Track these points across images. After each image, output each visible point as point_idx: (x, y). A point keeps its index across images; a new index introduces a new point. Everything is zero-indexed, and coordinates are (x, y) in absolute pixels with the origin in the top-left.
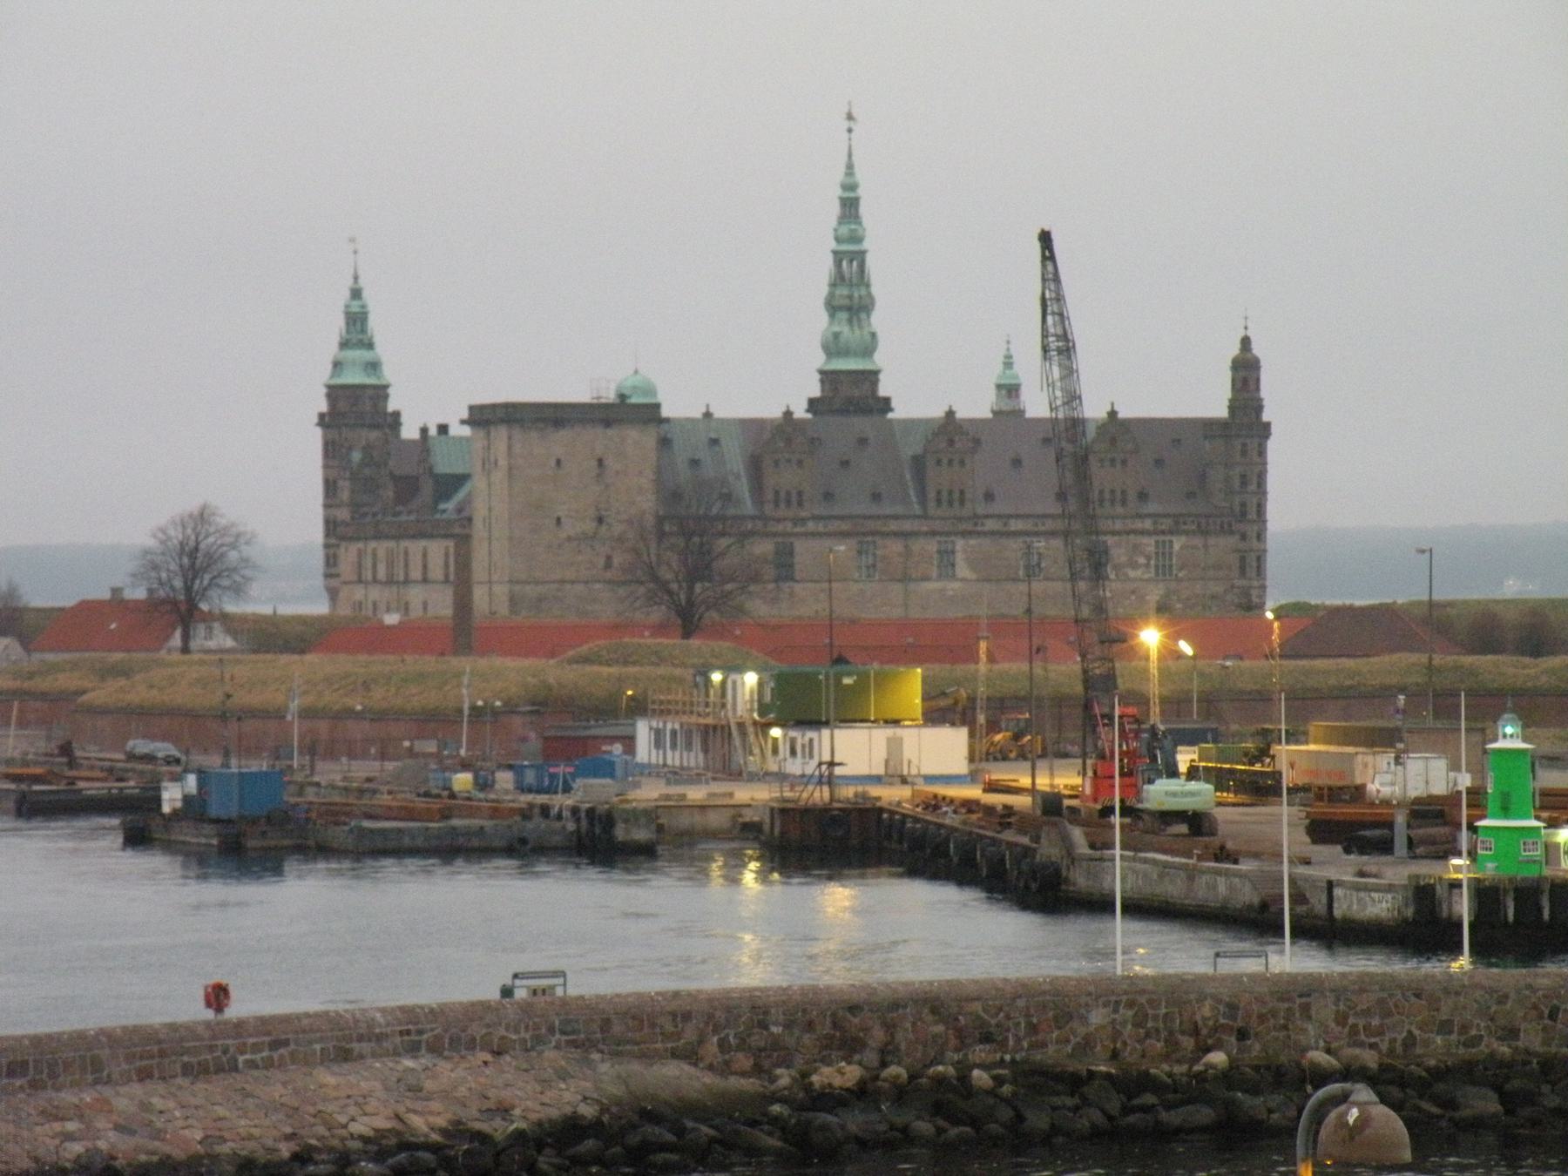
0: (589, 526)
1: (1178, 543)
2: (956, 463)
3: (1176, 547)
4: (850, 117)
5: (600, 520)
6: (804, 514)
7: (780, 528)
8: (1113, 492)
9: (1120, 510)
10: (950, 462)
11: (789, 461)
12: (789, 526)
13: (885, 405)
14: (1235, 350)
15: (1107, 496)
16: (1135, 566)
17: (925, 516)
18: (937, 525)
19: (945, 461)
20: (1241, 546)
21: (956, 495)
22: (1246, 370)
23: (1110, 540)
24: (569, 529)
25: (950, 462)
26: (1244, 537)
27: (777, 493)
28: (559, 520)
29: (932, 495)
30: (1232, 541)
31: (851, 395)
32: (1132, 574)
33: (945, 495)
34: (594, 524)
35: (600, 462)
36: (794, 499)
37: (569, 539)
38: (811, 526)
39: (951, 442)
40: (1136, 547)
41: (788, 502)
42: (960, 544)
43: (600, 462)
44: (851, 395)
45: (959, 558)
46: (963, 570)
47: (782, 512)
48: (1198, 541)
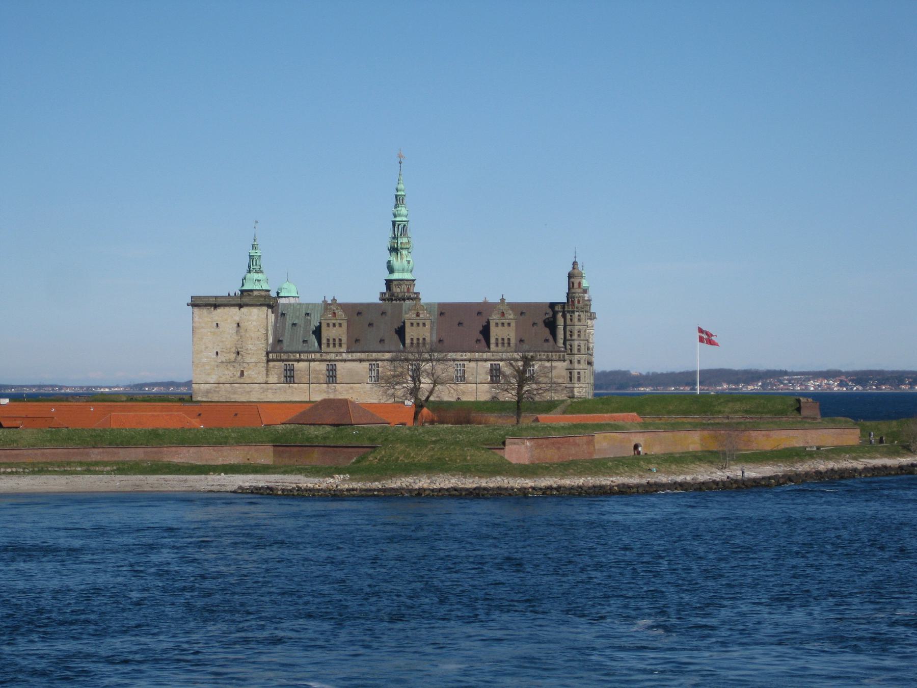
0: (233, 356)
2: (421, 325)
4: (400, 156)
5: (238, 353)
6: (342, 350)
7: (328, 357)
8: (503, 339)
10: (418, 324)
11: (334, 325)
12: (333, 356)
13: (417, 297)
14: (570, 269)
15: (500, 341)
19: (415, 324)
20: (570, 367)
22: (573, 277)
24: (222, 358)
25: (418, 324)
26: (571, 362)
27: (328, 340)
28: (217, 353)
30: (565, 364)
31: (397, 293)
34: (234, 355)
35: (238, 325)
36: (337, 342)
37: (222, 362)
38: (344, 356)
39: (418, 315)
41: (334, 345)
43: (238, 325)
44: (397, 293)
47: (331, 349)
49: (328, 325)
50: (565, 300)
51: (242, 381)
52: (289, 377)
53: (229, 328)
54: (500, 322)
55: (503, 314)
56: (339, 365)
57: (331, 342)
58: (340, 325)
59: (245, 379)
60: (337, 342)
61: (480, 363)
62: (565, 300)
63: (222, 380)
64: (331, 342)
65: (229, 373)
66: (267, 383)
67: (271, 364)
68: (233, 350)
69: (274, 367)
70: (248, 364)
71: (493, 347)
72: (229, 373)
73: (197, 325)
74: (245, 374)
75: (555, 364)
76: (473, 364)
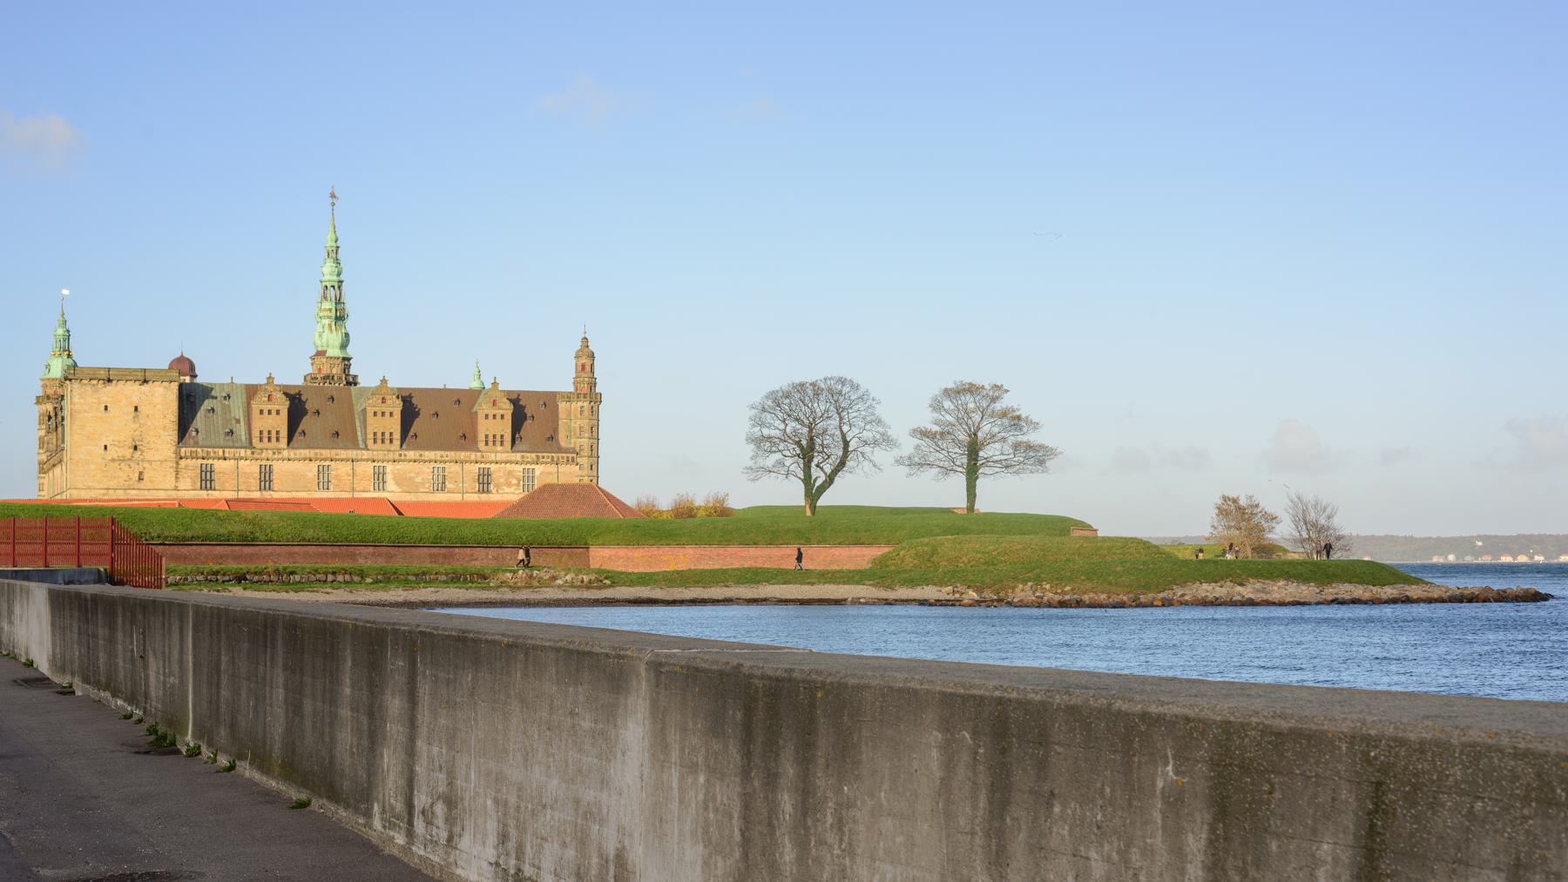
0: (128, 452)
1: (539, 469)
3: (537, 473)
9: (499, 448)
16: (509, 485)
17: (366, 448)
18: (375, 455)
21: (387, 436)
23: (493, 467)
29: (370, 436)
32: (507, 490)
33: (379, 436)
36: (274, 435)
37: (113, 460)
40: (510, 473)
42: (390, 467)
45: (389, 477)
46: (391, 485)
48: (553, 468)
49: (261, 412)
50: (572, 389)
51: (142, 485)
52: (207, 479)
53: (121, 413)
54: (491, 412)
55: (494, 403)
56: (278, 467)
57: (265, 434)
58: (278, 412)
59: (145, 484)
60: (274, 435)
61: (466, 466)
62: (572, 389)
63: (112, 484)
64: (265, 434)
65: (127, 473)
66: (176, 489)
67: (183, 463)
68: (130, 443)
69: (186, 467)
70: (150, 462)
71: (481, 445)
72: (127, 473)
73: (77, 407)
74: (146, 476)
75: (563, 468)
76: (455, 468)
